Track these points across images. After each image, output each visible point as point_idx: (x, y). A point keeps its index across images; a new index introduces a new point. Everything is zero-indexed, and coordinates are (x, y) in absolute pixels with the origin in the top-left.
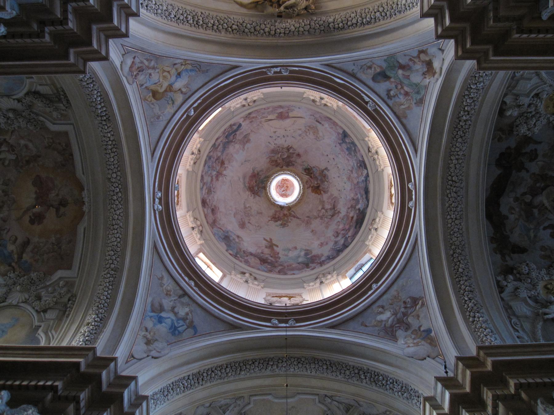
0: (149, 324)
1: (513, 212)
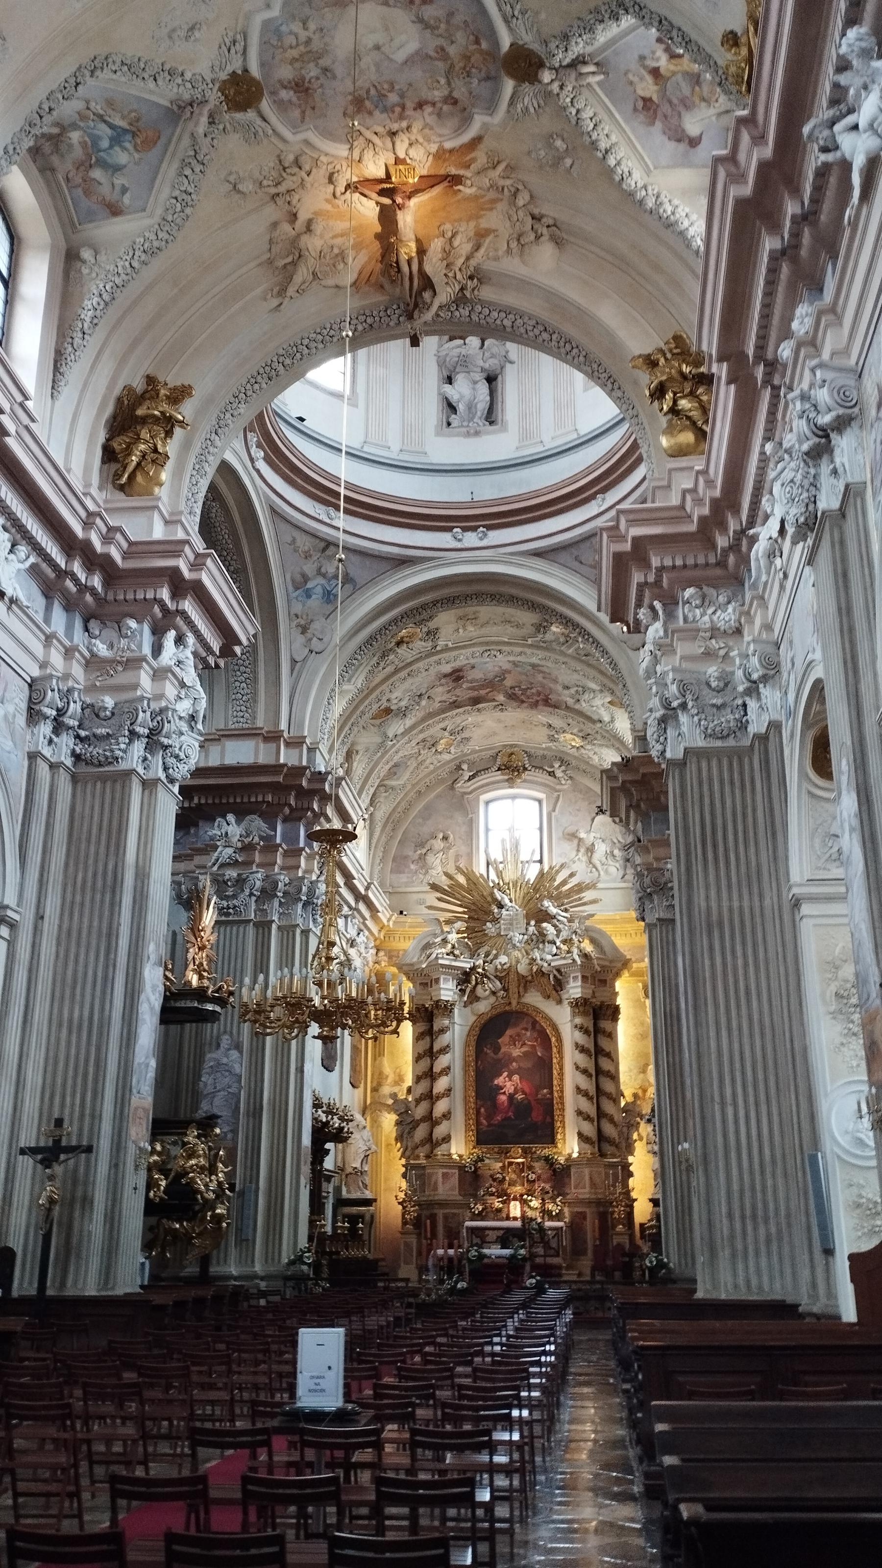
0: (297, 608)
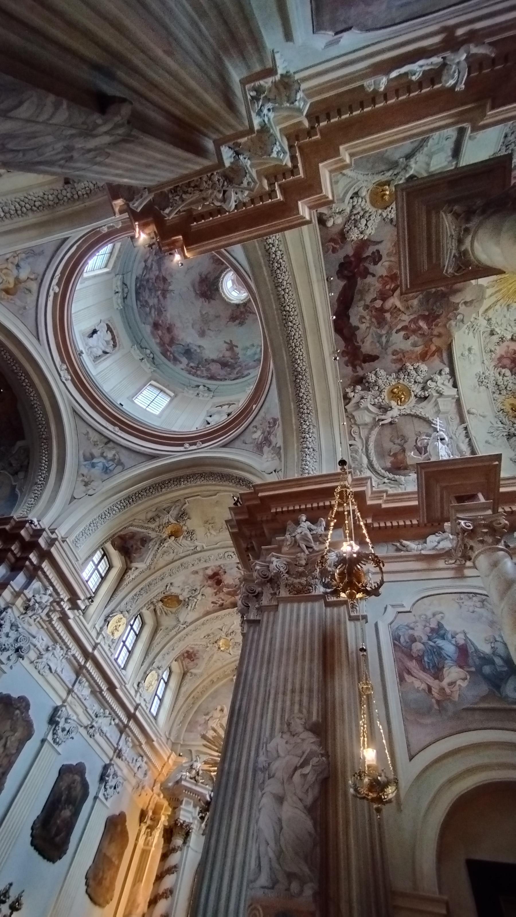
1: (364, 320)
